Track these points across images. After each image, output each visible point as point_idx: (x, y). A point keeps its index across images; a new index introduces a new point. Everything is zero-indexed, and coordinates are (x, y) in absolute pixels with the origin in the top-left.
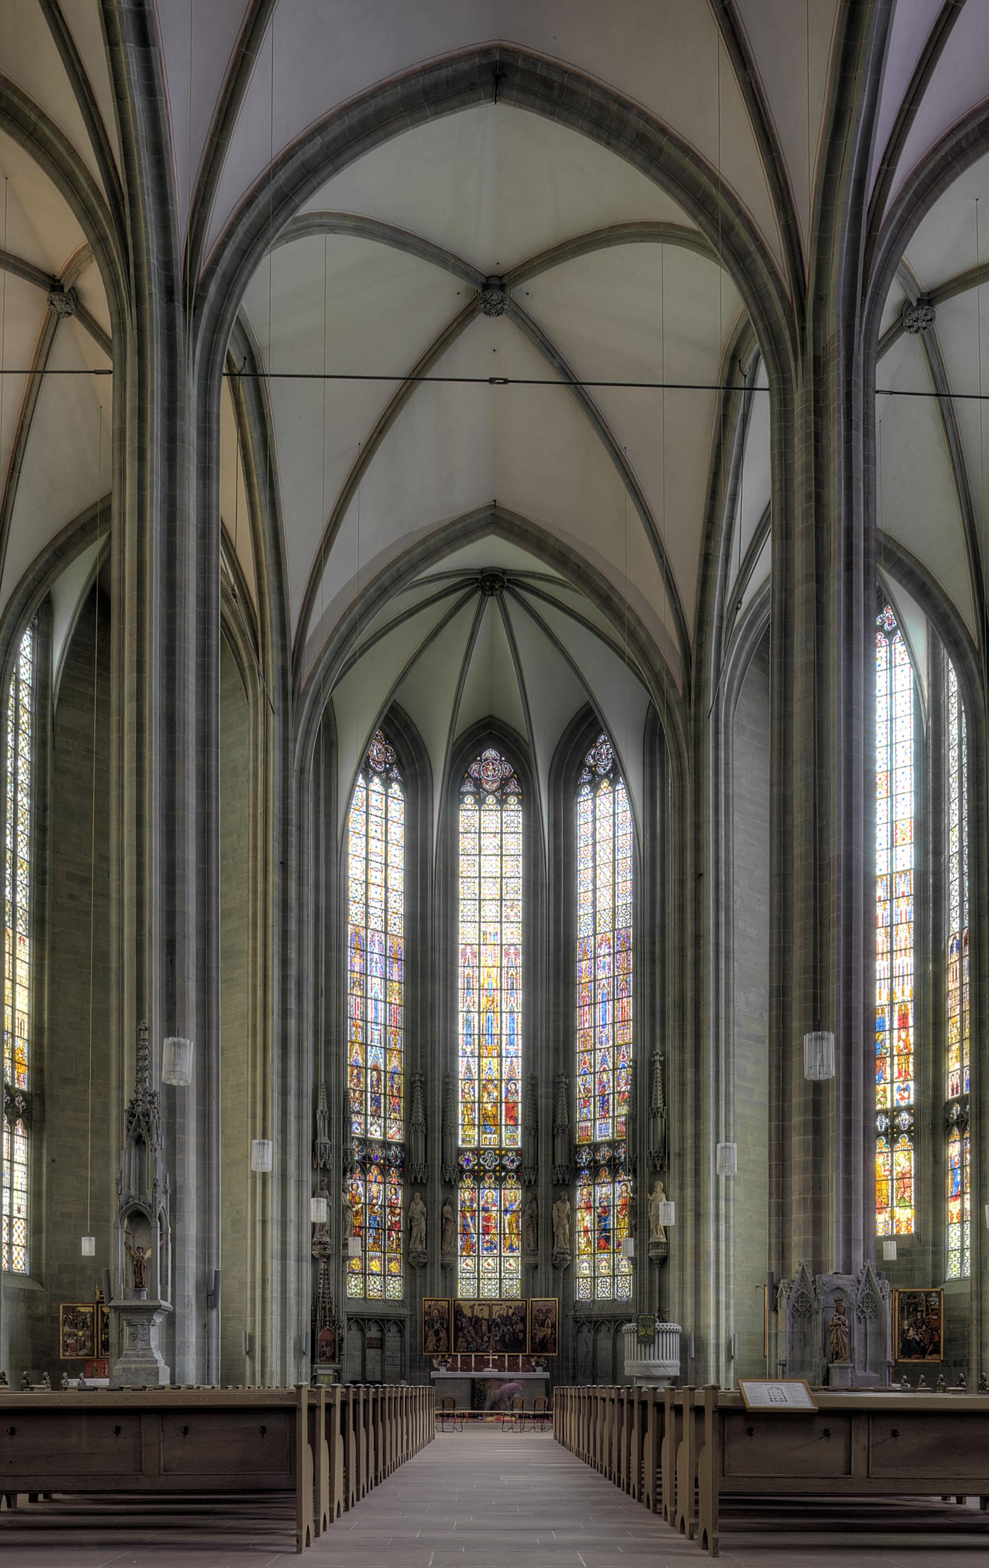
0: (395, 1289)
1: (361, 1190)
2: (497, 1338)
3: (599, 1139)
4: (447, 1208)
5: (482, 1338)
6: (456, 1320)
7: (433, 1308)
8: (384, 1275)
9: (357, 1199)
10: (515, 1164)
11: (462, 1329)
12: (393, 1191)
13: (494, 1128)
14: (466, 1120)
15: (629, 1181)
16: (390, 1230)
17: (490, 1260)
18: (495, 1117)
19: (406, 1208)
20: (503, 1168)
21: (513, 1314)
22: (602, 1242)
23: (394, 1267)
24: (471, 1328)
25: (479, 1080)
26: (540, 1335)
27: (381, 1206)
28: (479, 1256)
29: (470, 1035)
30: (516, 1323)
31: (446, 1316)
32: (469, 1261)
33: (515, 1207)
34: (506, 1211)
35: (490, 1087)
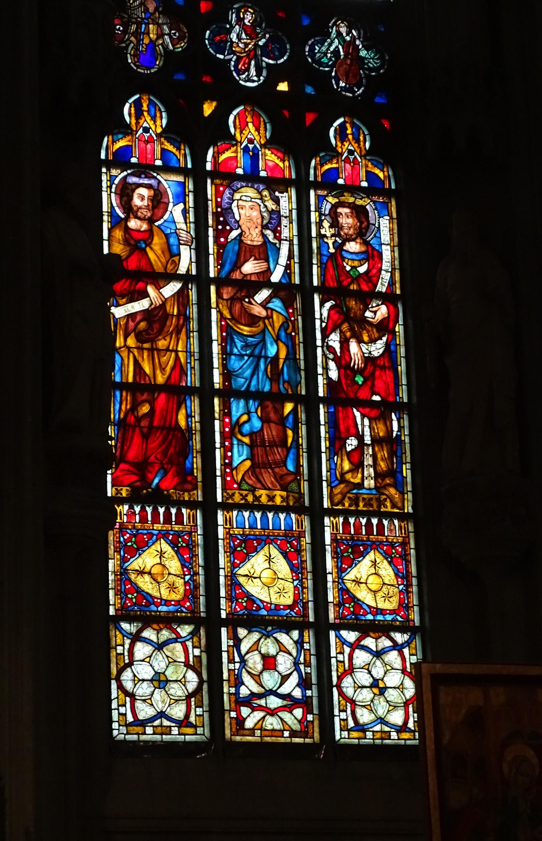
0: (381, 693)
1: (177, 216)
8: (317, 619)
9: (155, 255)
12: (347, 220)
16: (341, 397)
19: (415, 293)
23: (373, 581)
27: (282, 291)
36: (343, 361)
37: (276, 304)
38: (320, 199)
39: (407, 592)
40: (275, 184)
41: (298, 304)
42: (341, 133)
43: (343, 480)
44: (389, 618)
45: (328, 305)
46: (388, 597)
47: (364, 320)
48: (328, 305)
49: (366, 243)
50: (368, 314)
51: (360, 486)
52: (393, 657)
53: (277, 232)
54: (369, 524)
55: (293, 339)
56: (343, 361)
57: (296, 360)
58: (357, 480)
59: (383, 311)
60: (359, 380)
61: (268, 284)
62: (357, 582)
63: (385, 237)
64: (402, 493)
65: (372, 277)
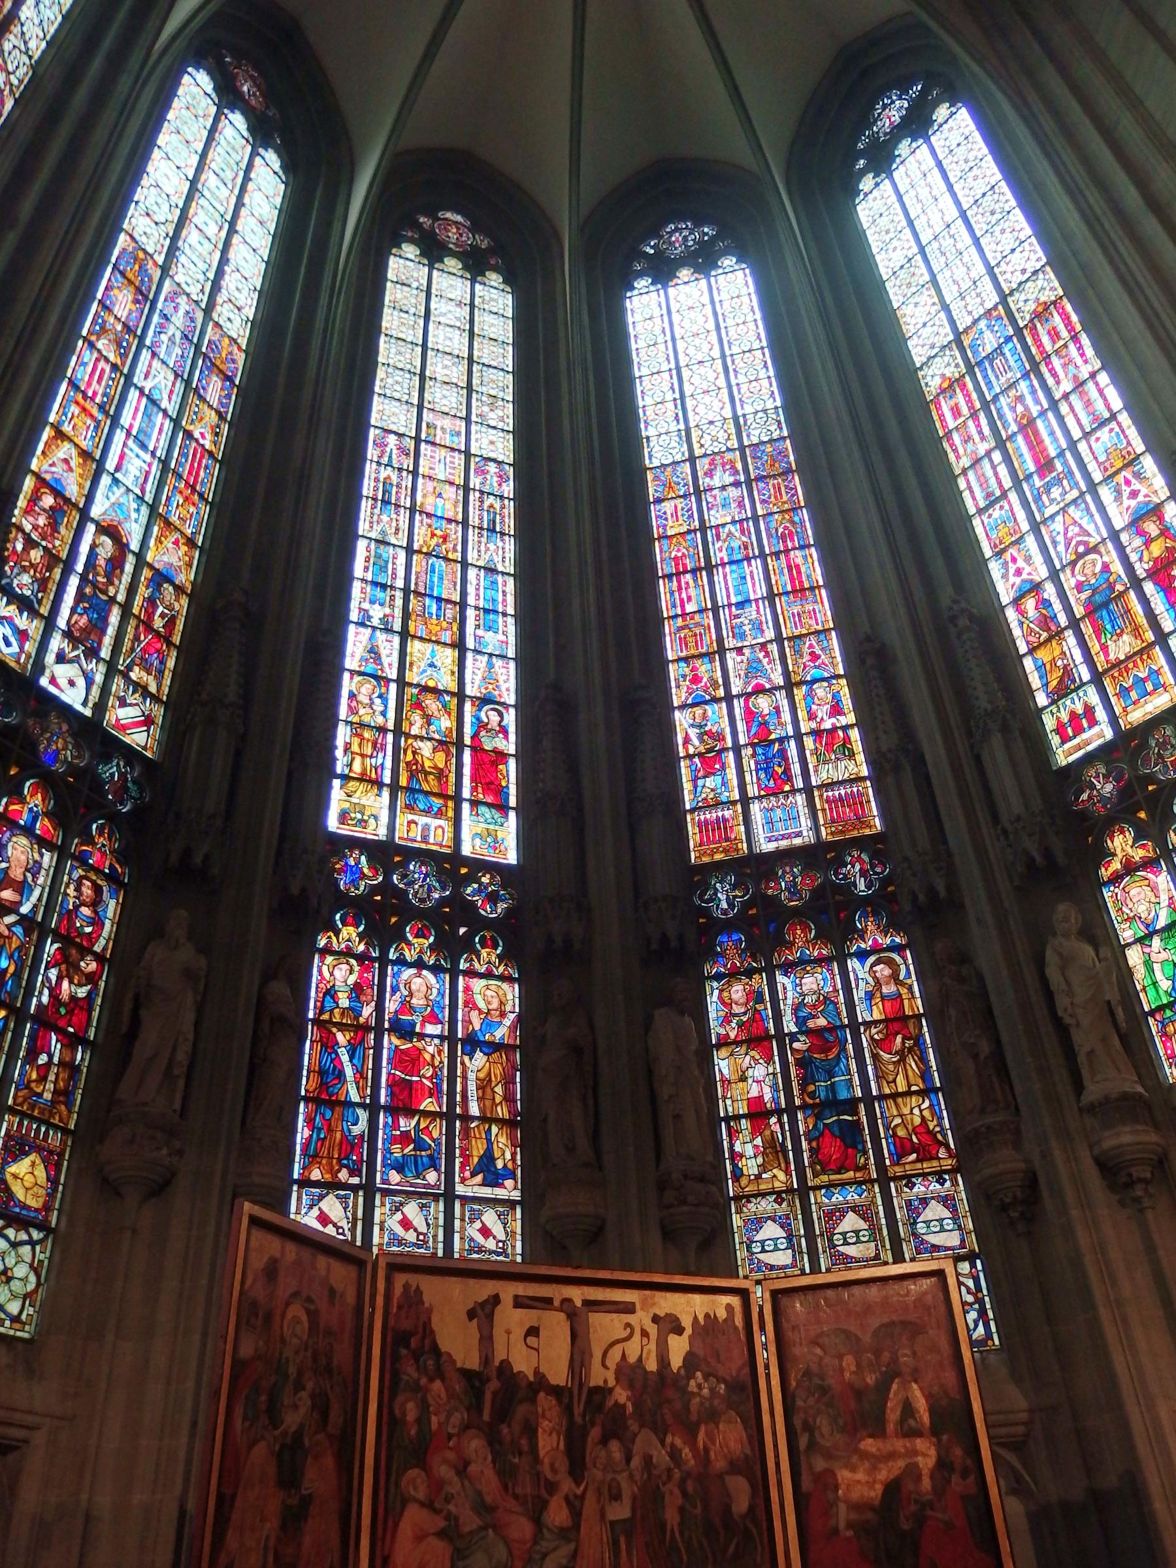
2: (620, 1511)
3: (768, 847)
4: (279, 988)
5: (537, 1512)
6: (392, 1385)
7: (287, 1284)
10: (501, 906)
11: (421, 1453)
12: (87, 891)
13: (437, 802)
14: (357, 767)
15: (899, 949)
16: (45, 1021)
17: (411, 1210)
18: (441, 774)
20: (466, 912)
21: (690, 1360)
22: (833, 1149)
24: (475, 1445)
25: (402, 682)
26: (859, 1483)
28: (369, 1189)
29: (384, 587)
30: (712, 1416)
31: (342, 1353)
32: (332, 1206)
33: (500, 1033)
34: (472, 1043)
35: (432, 704)
36: (55, 993)
37: (18, 930)
38: (72, 867)
39: (51, 1196)
40: (43, 842)
41: (35, 937)
42: (100, 830)
43: (28, 1087)
44: (32, 1214)
45: (56, 946)
46: (36, 1196)
47: (78, 968)
48: (56, 946)
49: (96, 912)
50: (82, 964)
51: (40, 1095)
52: (26, 1250)
53: (35, 877)
54: (38, 1130)
55: (23, 962)
56: (55, 993)
57: (20, 978)
58: (39, 1090)
59: (93, 966)
60: (63, 1011)
61: (17, 913)
62: (15, 1176)
63: (110, 914)
64: (70, 1112)
65: (92, 938)
